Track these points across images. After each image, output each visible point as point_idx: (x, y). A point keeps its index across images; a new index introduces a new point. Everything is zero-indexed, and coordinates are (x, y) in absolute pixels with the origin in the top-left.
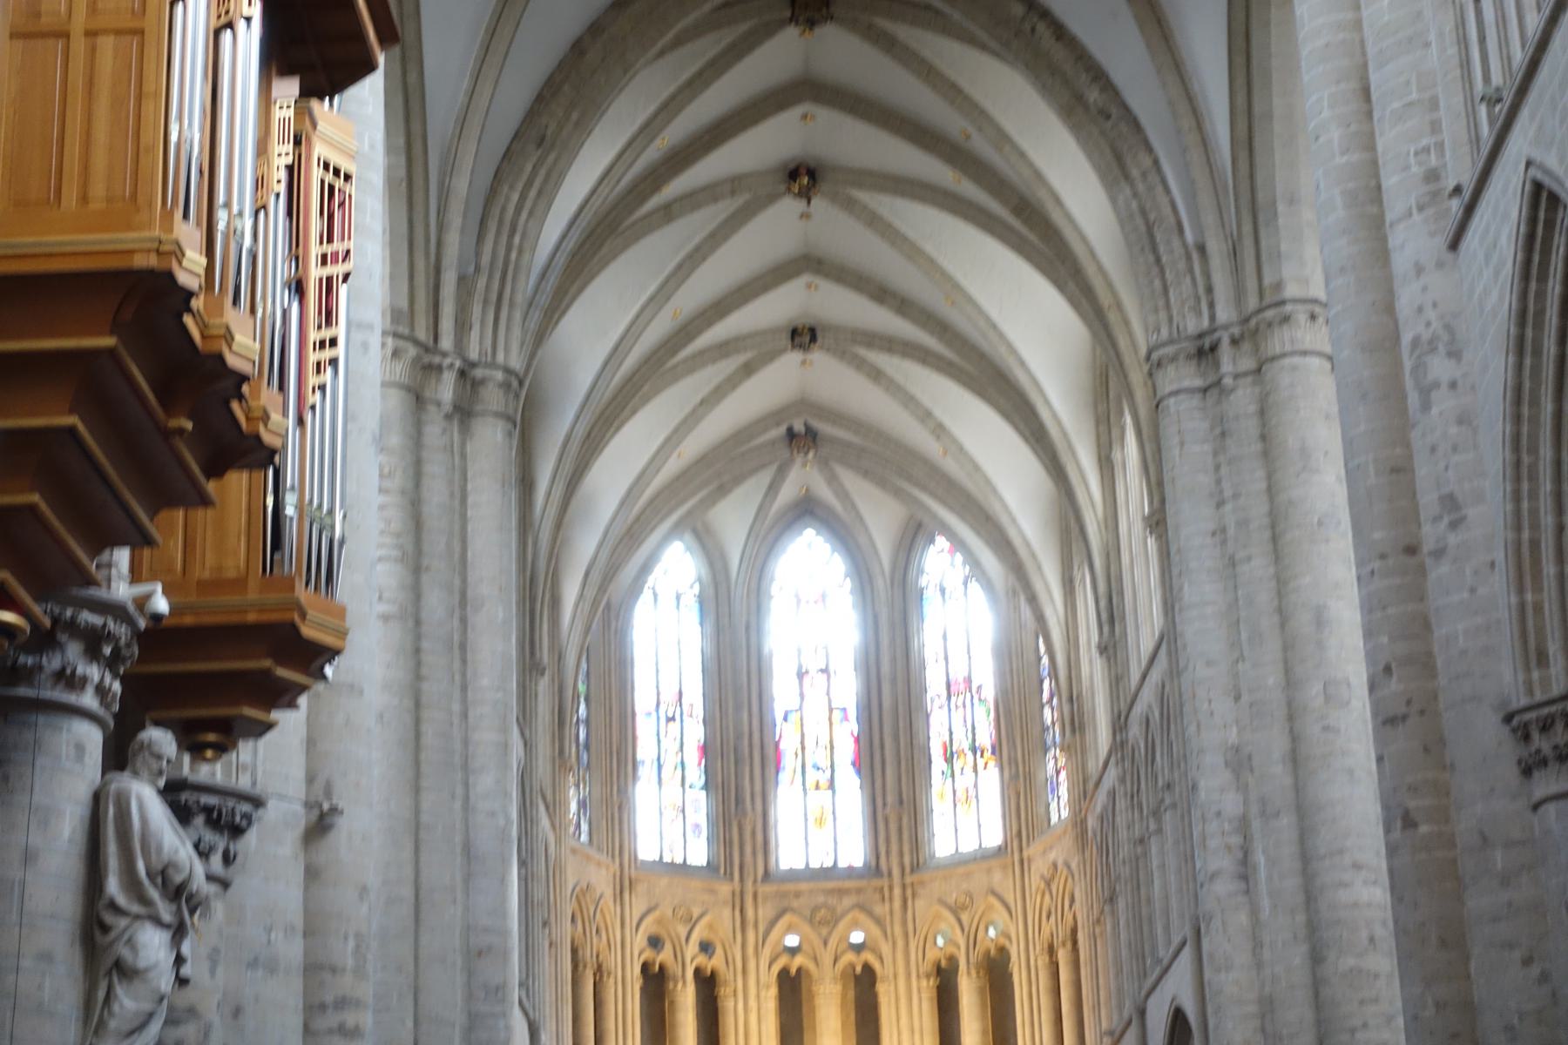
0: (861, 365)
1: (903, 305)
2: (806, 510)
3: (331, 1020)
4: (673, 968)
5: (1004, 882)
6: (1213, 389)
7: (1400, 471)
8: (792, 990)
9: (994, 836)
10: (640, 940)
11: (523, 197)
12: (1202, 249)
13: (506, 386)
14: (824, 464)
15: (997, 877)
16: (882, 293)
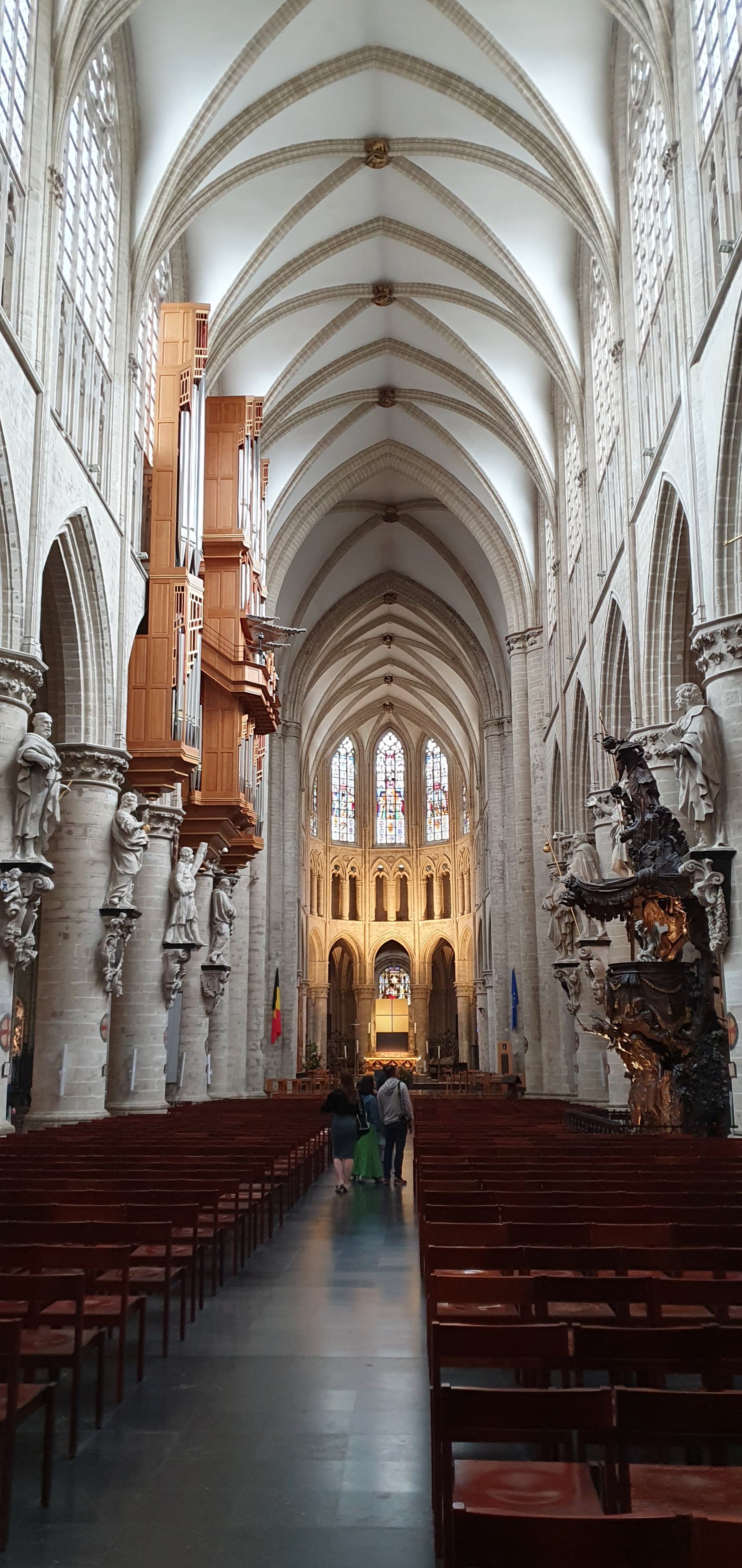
0: (406, 688)
1: (420, 675)
2: (389, 727)
3: (256, 930)
4: (342, 876)
5: (448, 851)
6: (501, 735)
7: (528, 798)
8: (380, 883)
9: (446, 836)
10: (332, 867)
11: (302, 669)
12: (500, 692)
13: (296, 728)
14: (394, 714)
15: (447, 850)
16: (413, 671)
